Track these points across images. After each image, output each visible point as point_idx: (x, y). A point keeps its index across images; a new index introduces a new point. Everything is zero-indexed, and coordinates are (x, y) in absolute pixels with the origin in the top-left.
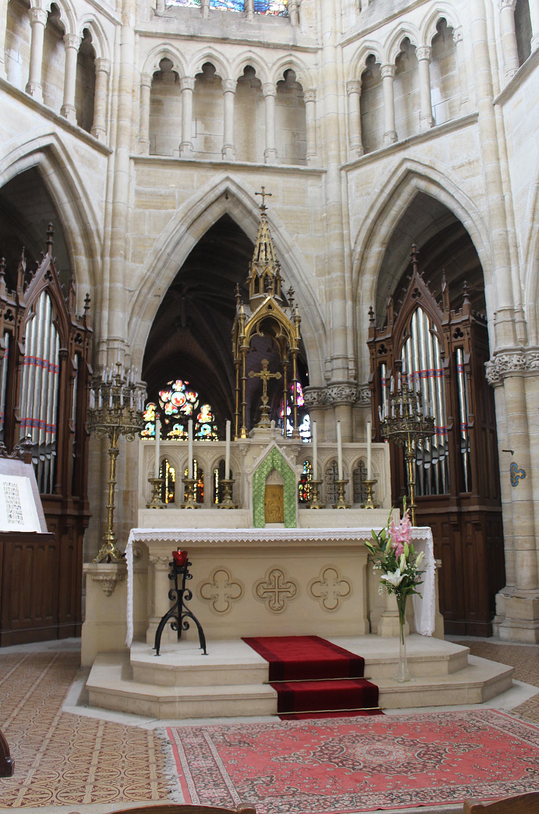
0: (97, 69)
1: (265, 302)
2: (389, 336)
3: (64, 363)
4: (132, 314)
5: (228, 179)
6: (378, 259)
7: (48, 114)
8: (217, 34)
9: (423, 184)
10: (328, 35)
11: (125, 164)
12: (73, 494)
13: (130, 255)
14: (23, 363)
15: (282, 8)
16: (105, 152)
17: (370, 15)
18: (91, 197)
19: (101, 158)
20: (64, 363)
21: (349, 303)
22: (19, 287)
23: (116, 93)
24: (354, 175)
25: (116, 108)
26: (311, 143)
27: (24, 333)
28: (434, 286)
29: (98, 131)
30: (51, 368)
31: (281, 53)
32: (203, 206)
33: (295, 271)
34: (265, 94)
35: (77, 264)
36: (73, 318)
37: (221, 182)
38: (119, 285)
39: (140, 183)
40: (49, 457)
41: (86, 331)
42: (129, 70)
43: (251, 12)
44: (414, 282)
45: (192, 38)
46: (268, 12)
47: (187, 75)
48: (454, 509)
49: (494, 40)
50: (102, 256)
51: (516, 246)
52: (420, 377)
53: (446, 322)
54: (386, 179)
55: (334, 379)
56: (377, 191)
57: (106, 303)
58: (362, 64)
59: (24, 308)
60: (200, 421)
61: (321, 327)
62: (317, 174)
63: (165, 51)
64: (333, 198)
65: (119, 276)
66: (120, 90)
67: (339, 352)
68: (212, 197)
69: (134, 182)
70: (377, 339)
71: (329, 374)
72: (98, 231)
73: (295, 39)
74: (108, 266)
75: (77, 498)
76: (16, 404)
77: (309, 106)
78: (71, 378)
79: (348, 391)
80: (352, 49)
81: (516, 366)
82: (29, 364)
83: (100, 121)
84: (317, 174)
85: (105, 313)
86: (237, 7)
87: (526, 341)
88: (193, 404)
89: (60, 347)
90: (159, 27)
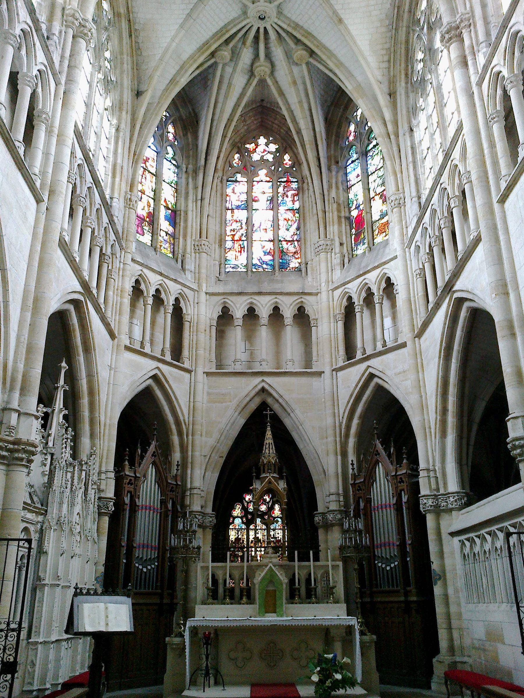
0: (184, 320)
1: (266, 480)
2: (362, 480)
3: (163, 506)
4: (205, 470)
5: (263, 381)
6: (358, 428)
7: (153, 358)
8: (255, 289)
9: (380, 382)
10: (323, 284)
11: (201, 377)
13: (204, 434)
14: (138, 510)
15: (297, 265)
16: (189, 371)
17: (348, 271)
18: (180, 401)
19: (187, 375)
20: (163, 506)
21: (339, 457)
22: (136, 465)
23: (195, 333)
24: (340, 374)
25: (195, 342)
26: (314, 354)
27: (139, 492)
28: (387, 449)
29: (184, 359)
30: (155, 510)
31: (295, 298)
32: (248, 399)
33: (306, 437)
34: (286, 324)
35: (172, 441)
36: (169, 477)
37: (259, 384)
38: (197, 454)
39: (210, 387)
40: (153, 566)
41: (177, 485)
42: (202, 318)
43: (277, 271)
44: (375, 446)
45: (240, 294)
46: (288, 268)
47: (238, 317)
48: (402, 599)
49: (415, 297)
50: (187, 436)
51: (430, 428)
52: (382, 508)
53: (394, 474)
54: (358, 378)
55: (331, 508)
56: (354, 385)
57: (189, 465)
58: (345, 303)
59: (139, 477)
60: (273, 515)
61: (323, 473)
62: (320, 374)
63: (225, 303)
64: (328, 389)
65: (197, 448)
67: (333, 490)
68: (253, 393)
69: (206, 387)
70: (357, 482)
71: (327, 504)
72: (184, 420)
73: (303, 288)
74: (190, 442)
77: (314, 329)
78: (167, 516)
79: (339, 516)
80: (338, 293)
81: (431, 506)
82: (142, 510)
83: (186, 353)
84: (320, 374)
85: (189, 472)
86: (269, 267)
87: (438, 490)
88: (268, 503)
89: (161, 497)
90: (220, 289)
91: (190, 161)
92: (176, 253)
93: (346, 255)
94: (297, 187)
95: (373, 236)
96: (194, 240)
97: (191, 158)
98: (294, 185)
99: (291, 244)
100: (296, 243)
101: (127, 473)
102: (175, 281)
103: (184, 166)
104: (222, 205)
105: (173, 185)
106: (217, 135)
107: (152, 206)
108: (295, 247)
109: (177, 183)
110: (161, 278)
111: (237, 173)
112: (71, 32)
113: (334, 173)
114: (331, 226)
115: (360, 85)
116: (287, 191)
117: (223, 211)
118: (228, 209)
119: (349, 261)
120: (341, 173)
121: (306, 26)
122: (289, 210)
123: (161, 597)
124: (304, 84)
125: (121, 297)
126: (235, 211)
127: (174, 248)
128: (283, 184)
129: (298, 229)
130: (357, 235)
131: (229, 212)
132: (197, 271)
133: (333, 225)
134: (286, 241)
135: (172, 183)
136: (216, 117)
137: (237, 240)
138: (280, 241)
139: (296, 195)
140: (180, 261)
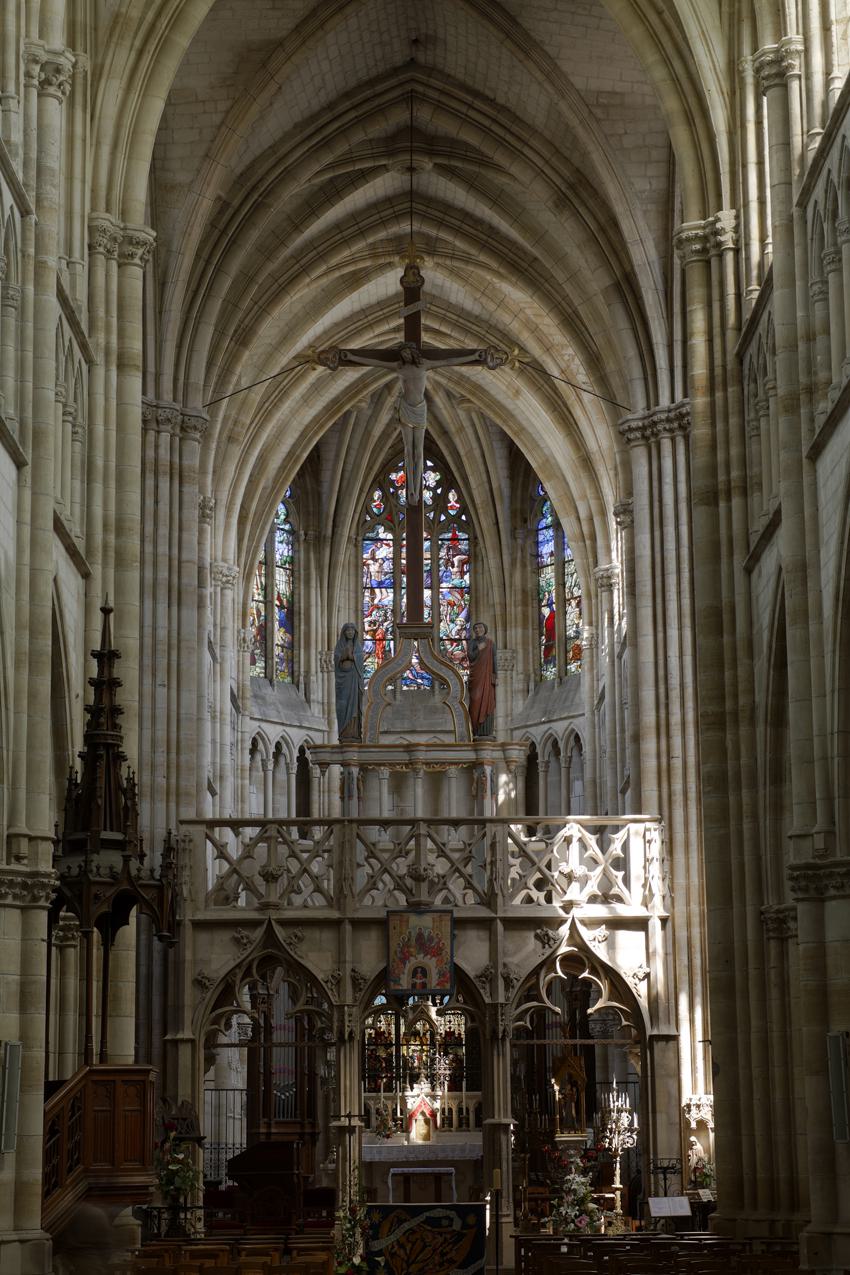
8: (407, 726)
12: (308, 1117)
23: (326, 794)
43: (437, 692)
66: (329, 791)
75: (311, 1120)
76: (271, 1061)
78: (304, 1036)
86: (426, 682)
91: (311, 523)
92: (296, 674)
93: (532, 676)
94: (467, 548)
95: (566, 660)
96: (321, 653)
97: (311, 517)
98: (463, 546)
99: (457, 646)
100: (464, 642)
101: (261, 992)
102: (301, 727)
103: (302, 532)
104: (357, 582)
105: (287, 566)
106: (350, 495)
107: (263, 614)
108: (462, 650)
109: (292, 562)
110: (281, 728)
111: (379, 524)
112: (219, 589)
113: (520, 541)
114: (513, 629)
115: (547, 460)
116: (454, 556)
117: (360, 591)
118: (366, 588)
119: (536, 686)
120: (529, 542)
121: (473, 379)
122: (456, 587)
123: (302, 1126)
124: (473, 425)
125: (242, 778)
126: (377, 591)
127: (292, 667)
128: (447, 543)
129: (468, 619)
130: (549, 649)
132: (326, 701)
133: (516, 626)
134: (450, 640)
135: (285, 562)
136: (349, 467)
137: (379, 640)
138: (442, 639)
139: (465, 563)
140: (302, 686)
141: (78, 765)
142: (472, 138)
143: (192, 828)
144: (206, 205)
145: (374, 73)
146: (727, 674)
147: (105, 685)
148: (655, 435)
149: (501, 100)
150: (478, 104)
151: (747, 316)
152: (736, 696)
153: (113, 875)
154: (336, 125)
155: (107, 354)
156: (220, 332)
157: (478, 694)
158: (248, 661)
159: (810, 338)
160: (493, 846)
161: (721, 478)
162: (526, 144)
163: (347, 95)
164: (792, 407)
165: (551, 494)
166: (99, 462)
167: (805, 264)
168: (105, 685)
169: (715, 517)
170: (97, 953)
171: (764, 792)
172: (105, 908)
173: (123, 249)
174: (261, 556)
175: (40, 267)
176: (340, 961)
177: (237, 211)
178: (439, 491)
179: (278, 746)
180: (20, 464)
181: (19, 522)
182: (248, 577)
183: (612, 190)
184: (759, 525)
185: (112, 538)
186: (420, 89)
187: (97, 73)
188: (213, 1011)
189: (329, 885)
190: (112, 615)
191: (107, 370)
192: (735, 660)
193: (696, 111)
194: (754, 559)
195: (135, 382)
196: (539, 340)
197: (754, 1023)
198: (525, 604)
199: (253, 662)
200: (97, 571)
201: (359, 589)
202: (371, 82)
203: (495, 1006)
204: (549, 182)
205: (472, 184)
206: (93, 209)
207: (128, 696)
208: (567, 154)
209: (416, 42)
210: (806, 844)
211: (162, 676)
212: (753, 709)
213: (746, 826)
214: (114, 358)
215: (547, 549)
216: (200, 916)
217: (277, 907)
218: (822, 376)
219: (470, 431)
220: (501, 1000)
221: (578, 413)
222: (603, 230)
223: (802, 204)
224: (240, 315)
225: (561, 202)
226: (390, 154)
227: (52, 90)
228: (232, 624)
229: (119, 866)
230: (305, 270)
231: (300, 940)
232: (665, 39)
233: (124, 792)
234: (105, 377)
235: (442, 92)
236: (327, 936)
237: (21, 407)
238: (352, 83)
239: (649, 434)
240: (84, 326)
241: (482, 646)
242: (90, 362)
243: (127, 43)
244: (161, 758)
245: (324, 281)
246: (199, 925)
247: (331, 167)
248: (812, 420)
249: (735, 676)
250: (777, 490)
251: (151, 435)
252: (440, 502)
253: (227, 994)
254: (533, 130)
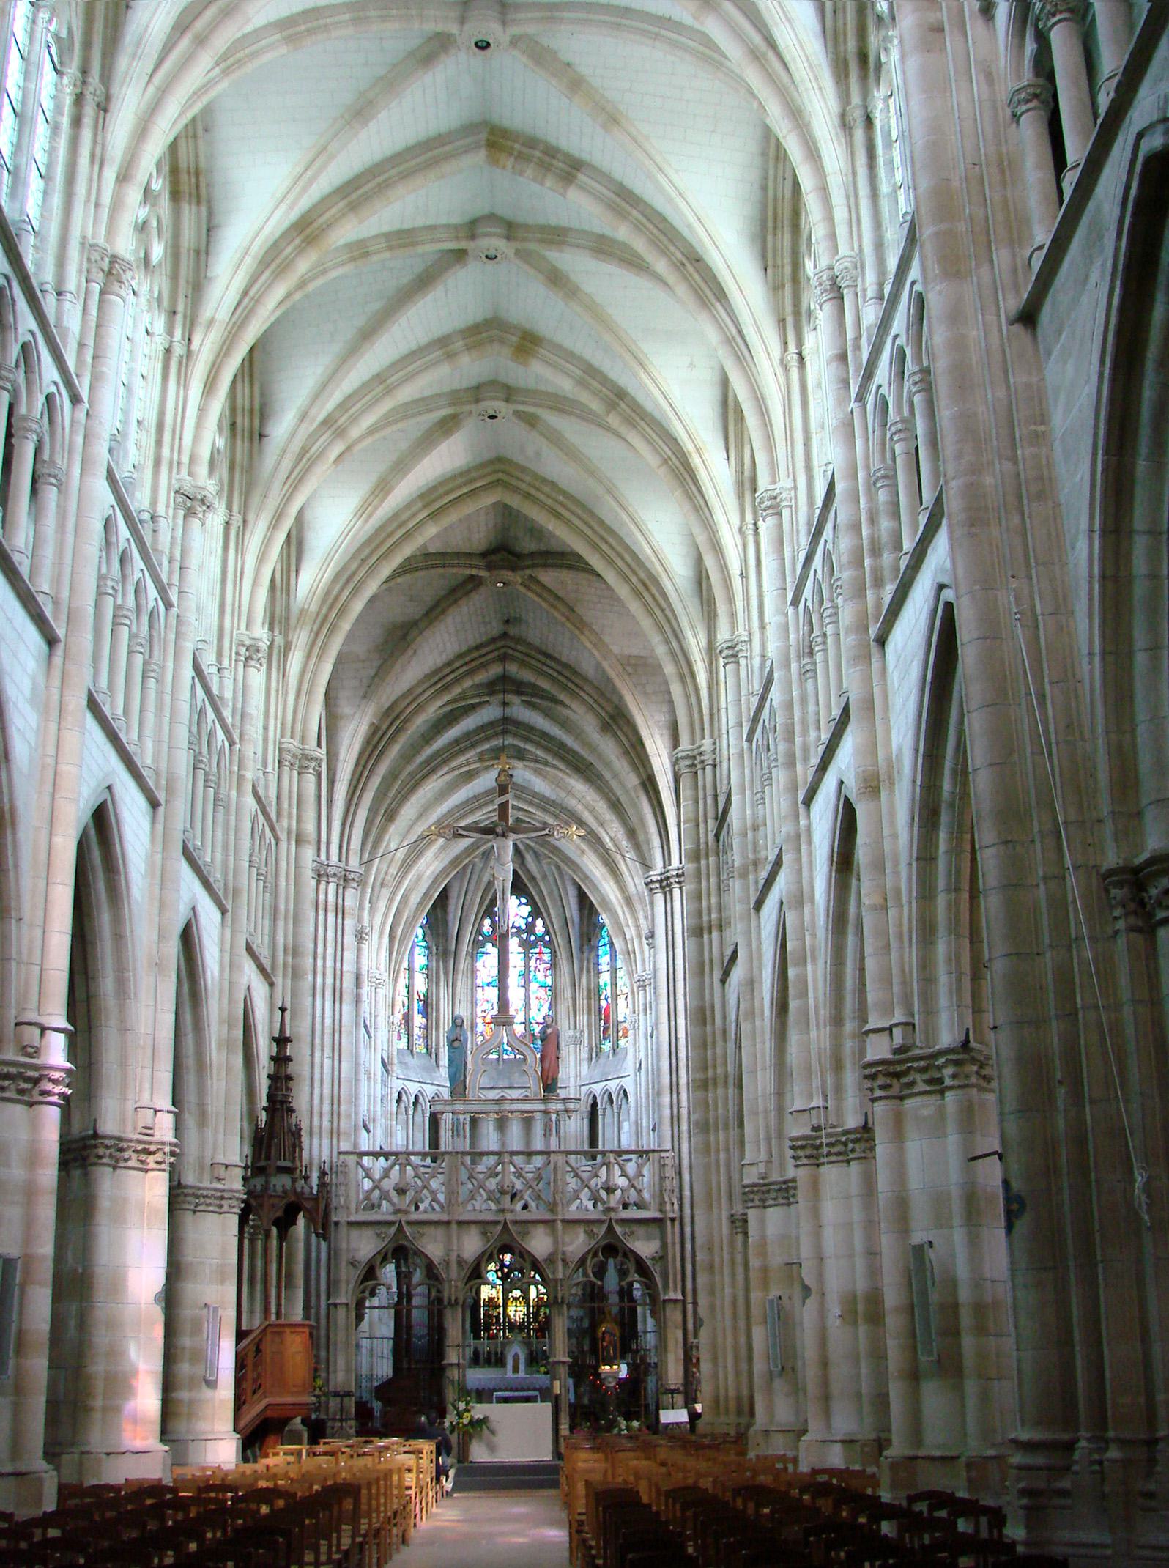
98: (547, 957)
109: (427, 968)
120: (593, 954)
130: (606, 1029)
131: (479, 990)
141: (263, 1115)
142: (545, 684)
143: (346, 1157)
144: (363, 729)
145: (479, 641)
146: (709, 1053)
147: (280, 1060)
148: (668, 885)
149: (564, 659)
150: (549, 662)
151: (720, 810)
152: (715, 1067)
153: (285, 1192)
154: (452, 676)
155: (289, 833)
156: (373, 811)
157: (547, 1064)
158: (395, 1037)
159: (755, 829)
160: (555, 1168)
161: (705, 918)
162: (582, 689)
163: (460, 656)
164: (744, 875)
165: (607, 922)
166: (282, 907)
167: (752, 780)
168: (280, 1060)
169: (701, 946)
170: (274, 1242)
171: (734, 1132)
172: (279, 1213)
173: (303, 763)
174: (405, 965)
175: (241, 778)
176: (448, 1251)
177: (385, 733)
178: (530, 919)
179: (416, 1097)
180: (224, 912)
181: (222, 951)
182: (395, 979)
183: (639, 720)
184: (729, 952)
185: (290, 959)
186: (511, 652)
187: (288, 646)
188: (362, 1282)
189: (441, 1197)
190: (288, 1014)
191: (289, 844)
192: (714, 1043)
193: (687, 674)
194: (726, 974)
195: (309, 853)
196: (596, 818)
197: (728, 1290)
198: (589, 998)
199: (399, 1039)
200: (279, 980)
201: (473, 987)
202: (478, 648)
203: (556, 1280)
204: (598, 715)
205: (547, 714)
206: (282, 737)
207: (300, 1067)
208: (608, 695)
209: (507, 622)
210: (754, 1169)
211: (327, 1052)
212: (726, 1077)
213: (722, 1156)
214: (294, 836)
215: (605, 960)
216: (352, 1218)
217: (406, 1212)
218: (763, 854)
219: (551, 878)
220: (560, 1276)
221: (623, 867)
222: (632, 745)
223: (749, 740)
224: (388, 801)
225: (606, 727)
226: (491, 693)
227: (253, 663)
228: (383, 1012)
229: (289, 1186)
230: (433, 771)
231: (423, 1235)
232: (666, 627)
233: (293, 1134)
234: (287, 849)
235: (526, 654)
236: (439, 1233)
237: (225, 873)
238: (464, 648)
239: (665, 884)
240: (273, 816)
241: (549, 1031)
242: (277, 839)
243: (308, 628)
244: (326, 1108)
245: (448, 777)
246: (350, 1224)
247: (450, 702)
248: (757, 882)
249: (715, 1054)
250: (736, 934)
251: (323, 885)
252: (530, 928)
253: (370, 1273)
254: (585, 679)
